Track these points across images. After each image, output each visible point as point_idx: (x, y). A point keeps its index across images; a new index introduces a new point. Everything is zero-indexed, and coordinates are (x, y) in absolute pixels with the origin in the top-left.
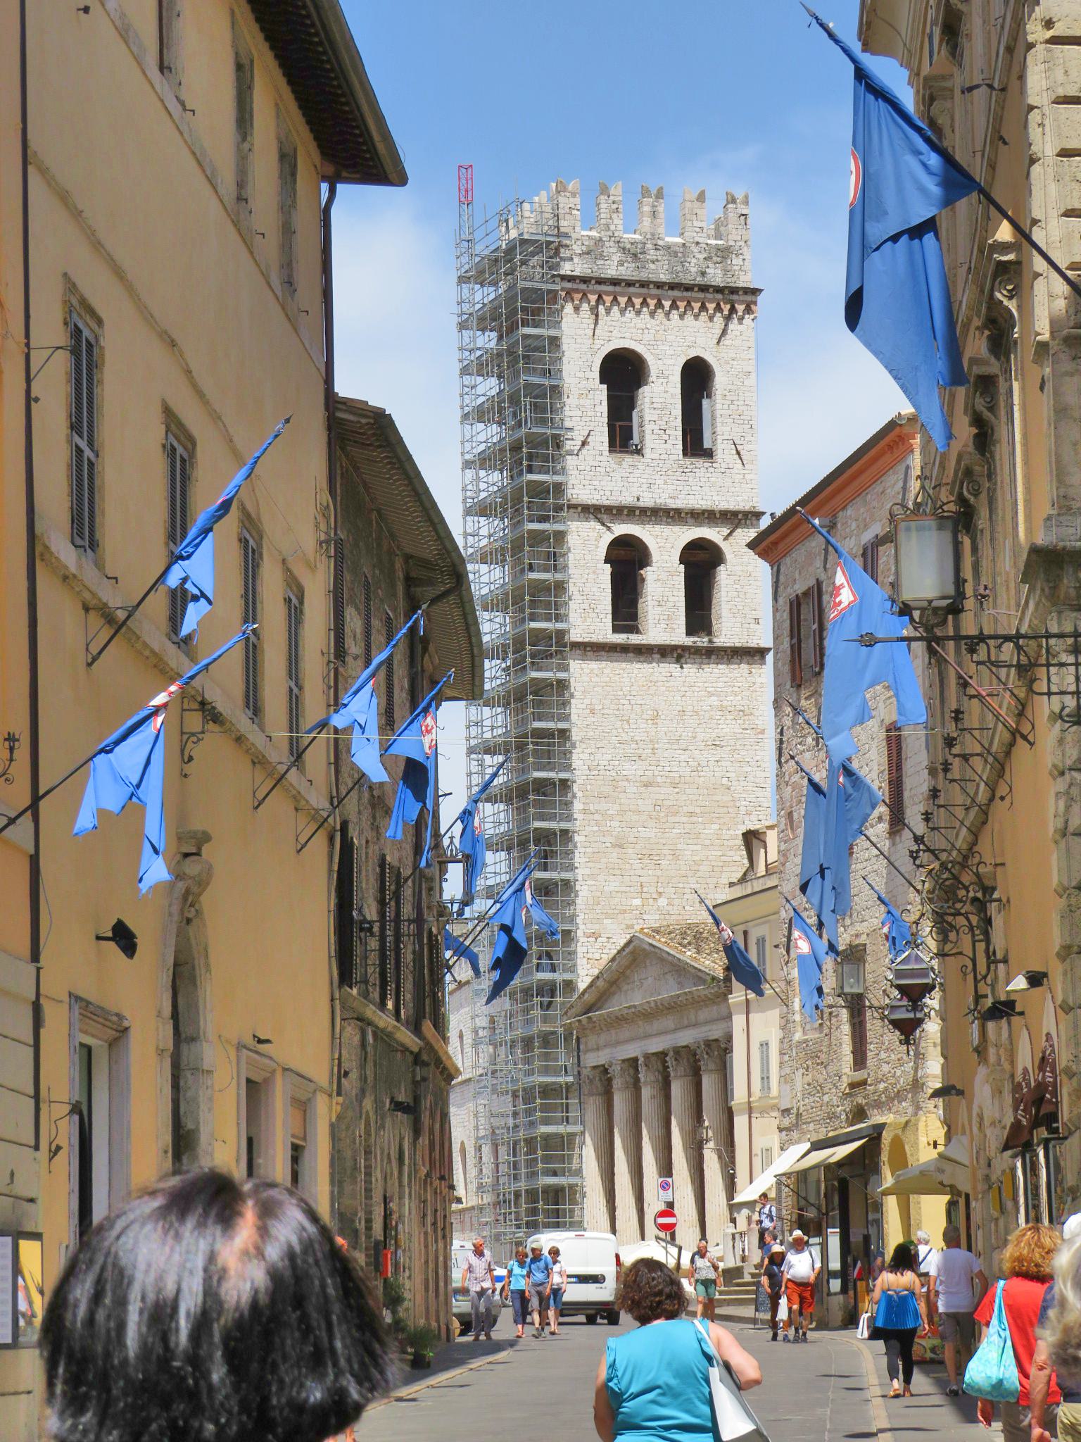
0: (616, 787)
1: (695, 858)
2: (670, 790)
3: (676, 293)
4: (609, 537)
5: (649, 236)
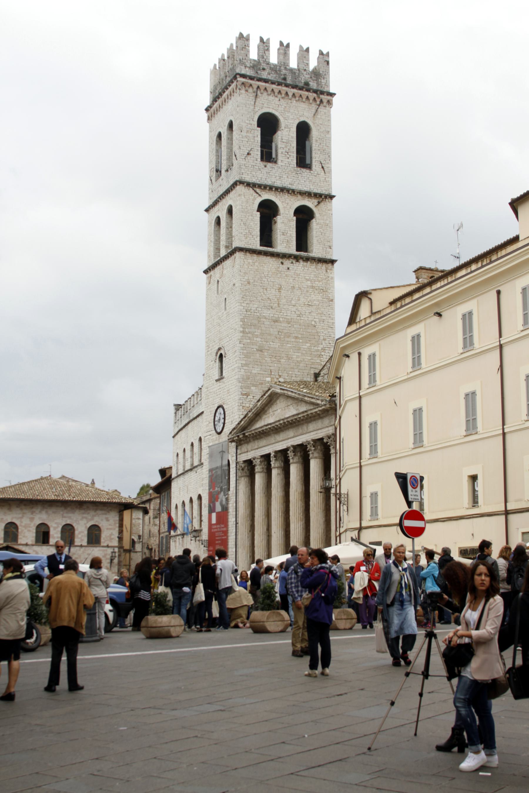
0: (259, 321)
1: (299, 359)
2: (286, 325)
3: (295, 91)
4: (259, 200)
5: (282, 64)
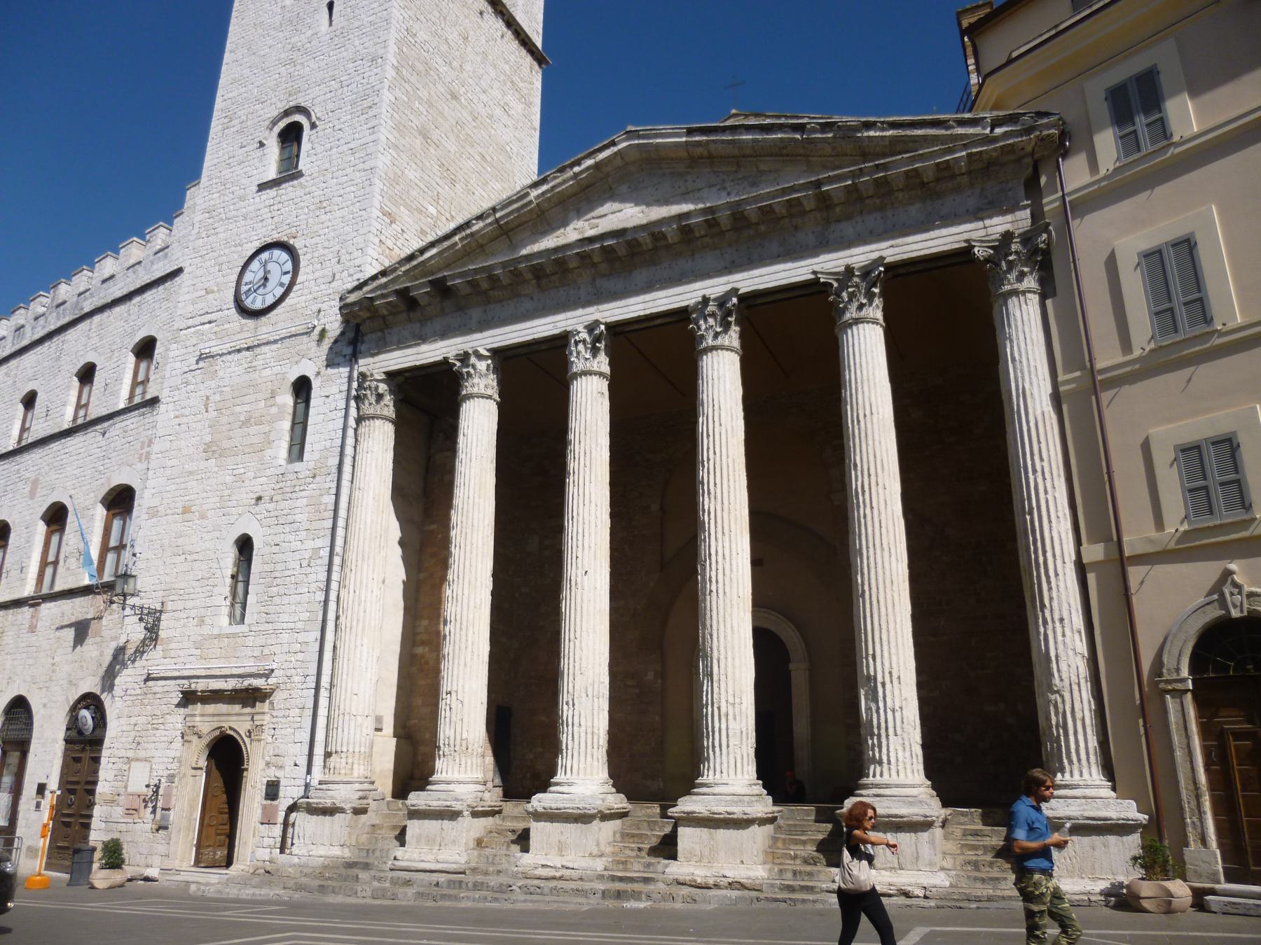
2: (470, 119)
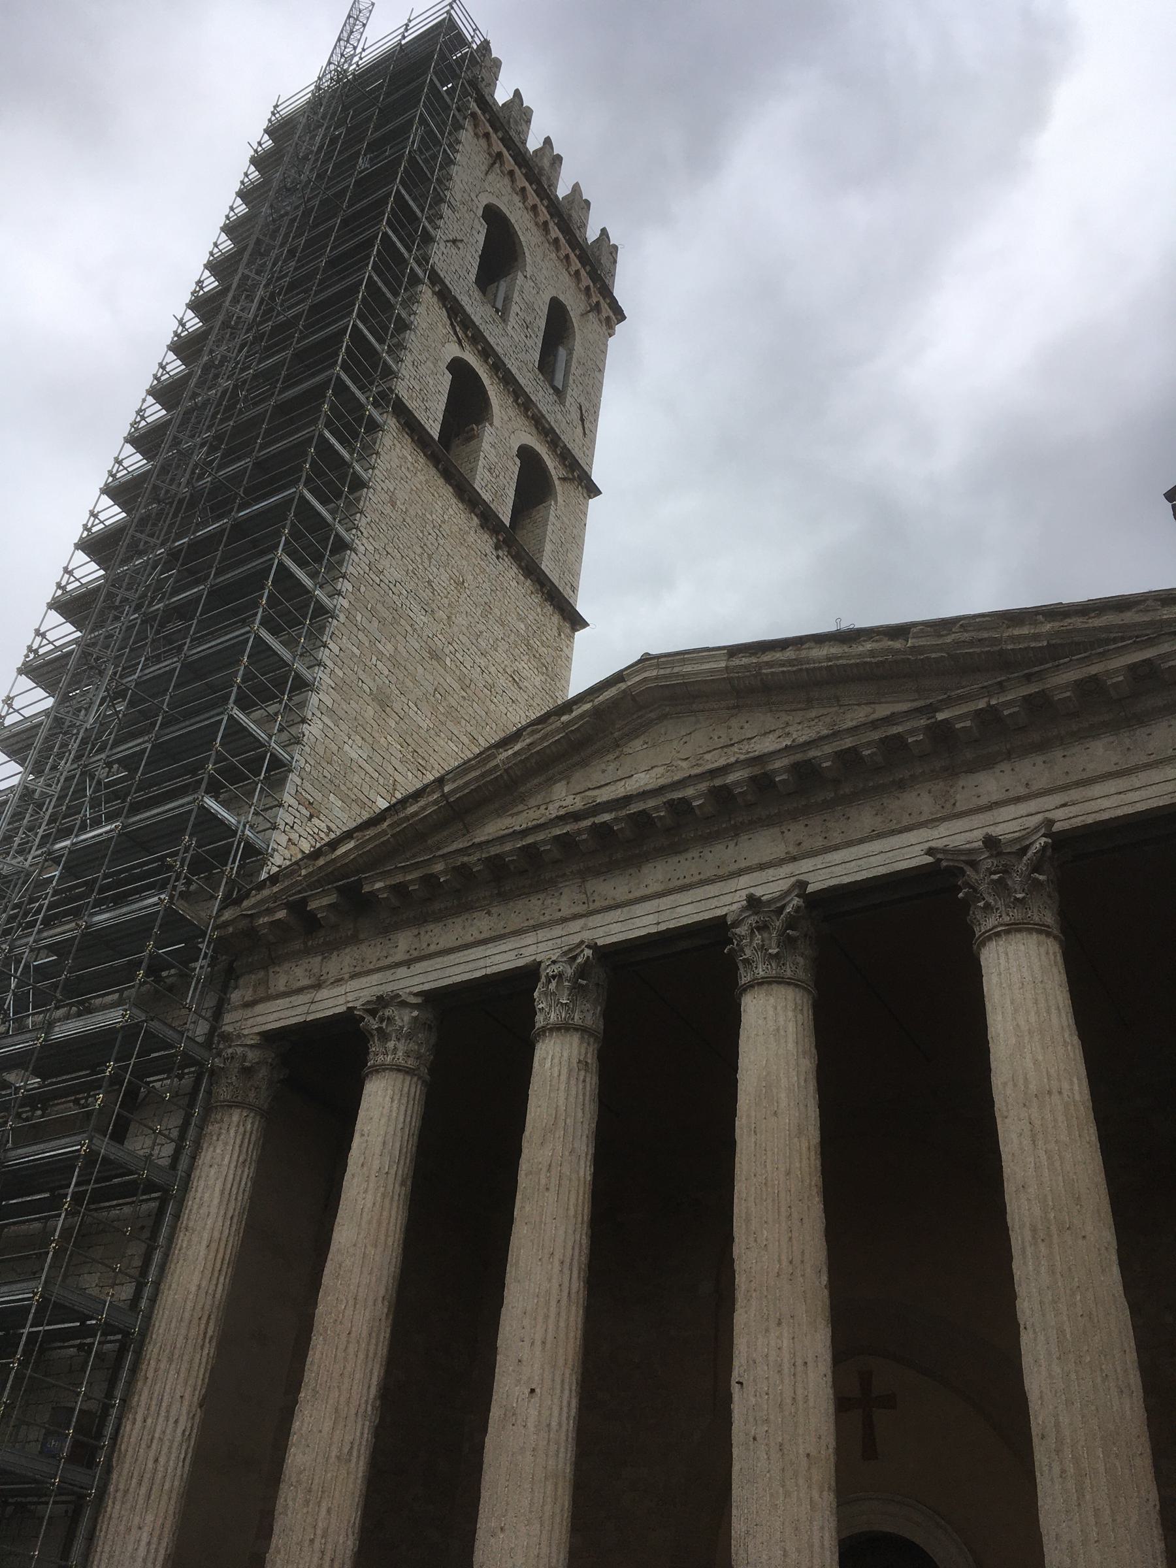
2: (456, 686)
